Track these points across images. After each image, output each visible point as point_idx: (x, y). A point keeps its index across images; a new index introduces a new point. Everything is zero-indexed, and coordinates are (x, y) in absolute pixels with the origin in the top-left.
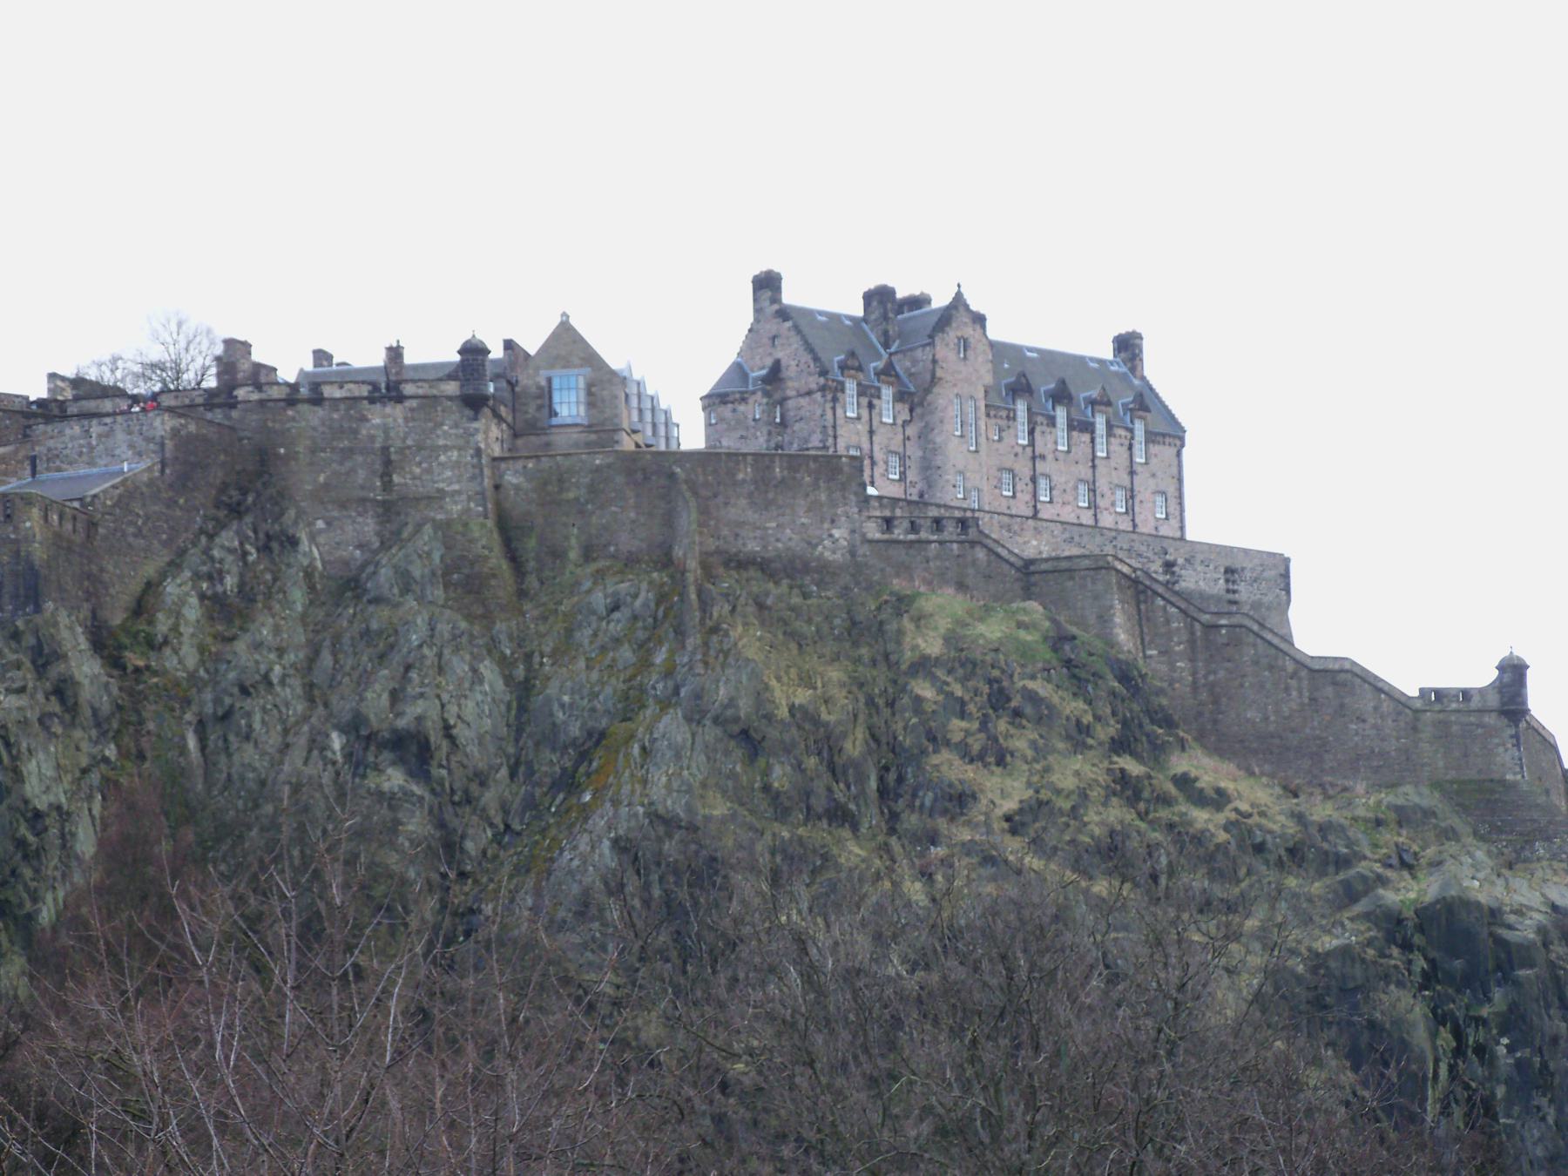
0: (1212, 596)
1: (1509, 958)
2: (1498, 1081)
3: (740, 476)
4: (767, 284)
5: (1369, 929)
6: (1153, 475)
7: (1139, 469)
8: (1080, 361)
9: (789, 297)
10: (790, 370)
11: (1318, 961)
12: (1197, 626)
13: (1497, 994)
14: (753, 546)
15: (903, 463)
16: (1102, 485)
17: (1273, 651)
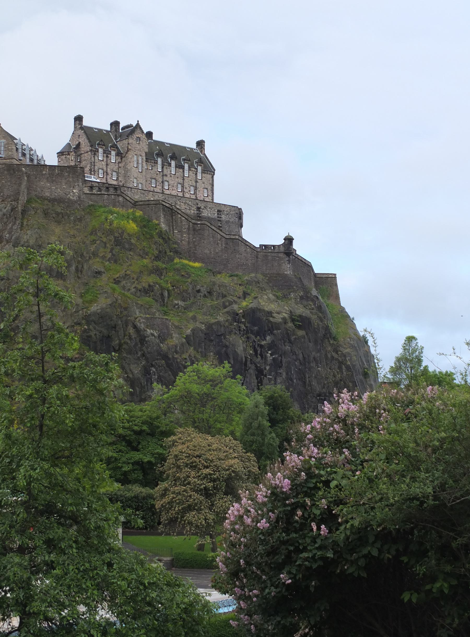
0: (213, 218)
1: (272, 327)
2: (267, 365)
3: (44, 172)
4: (79, 119)
6: (204, 183)
7: (199, 181)
8: (184, 149)
10: (83, 145)
11: (209, 326)
13: (268, 338)
14: (47, 194)
15: (118, 175)
16: (186, 185)
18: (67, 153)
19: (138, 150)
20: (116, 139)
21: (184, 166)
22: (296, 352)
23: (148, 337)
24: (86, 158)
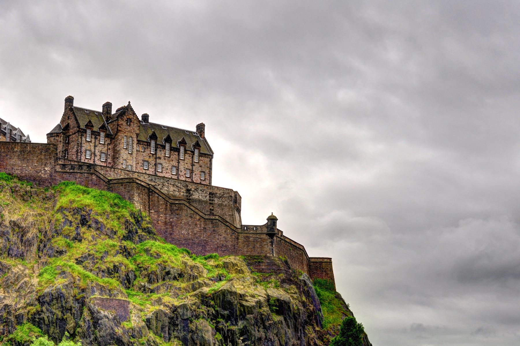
1: (245, 311)
3: (16, 150)
4: (69, 100)
5: (196, 299)
6: (201, 166)
9: (76, 104)
11: (175, 309)
12: (168, 204)
14: (18, 172)
16: (181, 168)
17: (193, 212)
18: (56, 134)
19: (129, 131)
20: (107, 121)
21: (179, 149)
22: (271, 339)
23: (101, 319)
24: (74, 140)
